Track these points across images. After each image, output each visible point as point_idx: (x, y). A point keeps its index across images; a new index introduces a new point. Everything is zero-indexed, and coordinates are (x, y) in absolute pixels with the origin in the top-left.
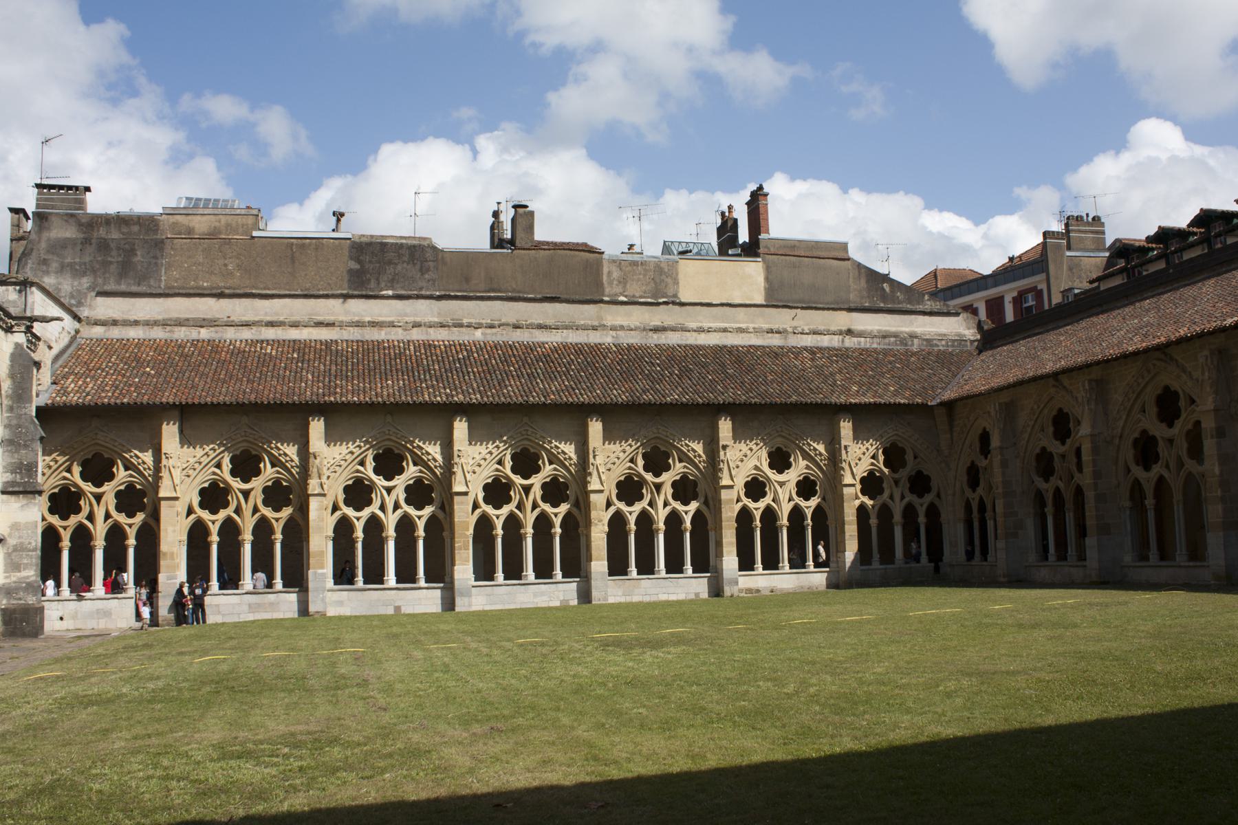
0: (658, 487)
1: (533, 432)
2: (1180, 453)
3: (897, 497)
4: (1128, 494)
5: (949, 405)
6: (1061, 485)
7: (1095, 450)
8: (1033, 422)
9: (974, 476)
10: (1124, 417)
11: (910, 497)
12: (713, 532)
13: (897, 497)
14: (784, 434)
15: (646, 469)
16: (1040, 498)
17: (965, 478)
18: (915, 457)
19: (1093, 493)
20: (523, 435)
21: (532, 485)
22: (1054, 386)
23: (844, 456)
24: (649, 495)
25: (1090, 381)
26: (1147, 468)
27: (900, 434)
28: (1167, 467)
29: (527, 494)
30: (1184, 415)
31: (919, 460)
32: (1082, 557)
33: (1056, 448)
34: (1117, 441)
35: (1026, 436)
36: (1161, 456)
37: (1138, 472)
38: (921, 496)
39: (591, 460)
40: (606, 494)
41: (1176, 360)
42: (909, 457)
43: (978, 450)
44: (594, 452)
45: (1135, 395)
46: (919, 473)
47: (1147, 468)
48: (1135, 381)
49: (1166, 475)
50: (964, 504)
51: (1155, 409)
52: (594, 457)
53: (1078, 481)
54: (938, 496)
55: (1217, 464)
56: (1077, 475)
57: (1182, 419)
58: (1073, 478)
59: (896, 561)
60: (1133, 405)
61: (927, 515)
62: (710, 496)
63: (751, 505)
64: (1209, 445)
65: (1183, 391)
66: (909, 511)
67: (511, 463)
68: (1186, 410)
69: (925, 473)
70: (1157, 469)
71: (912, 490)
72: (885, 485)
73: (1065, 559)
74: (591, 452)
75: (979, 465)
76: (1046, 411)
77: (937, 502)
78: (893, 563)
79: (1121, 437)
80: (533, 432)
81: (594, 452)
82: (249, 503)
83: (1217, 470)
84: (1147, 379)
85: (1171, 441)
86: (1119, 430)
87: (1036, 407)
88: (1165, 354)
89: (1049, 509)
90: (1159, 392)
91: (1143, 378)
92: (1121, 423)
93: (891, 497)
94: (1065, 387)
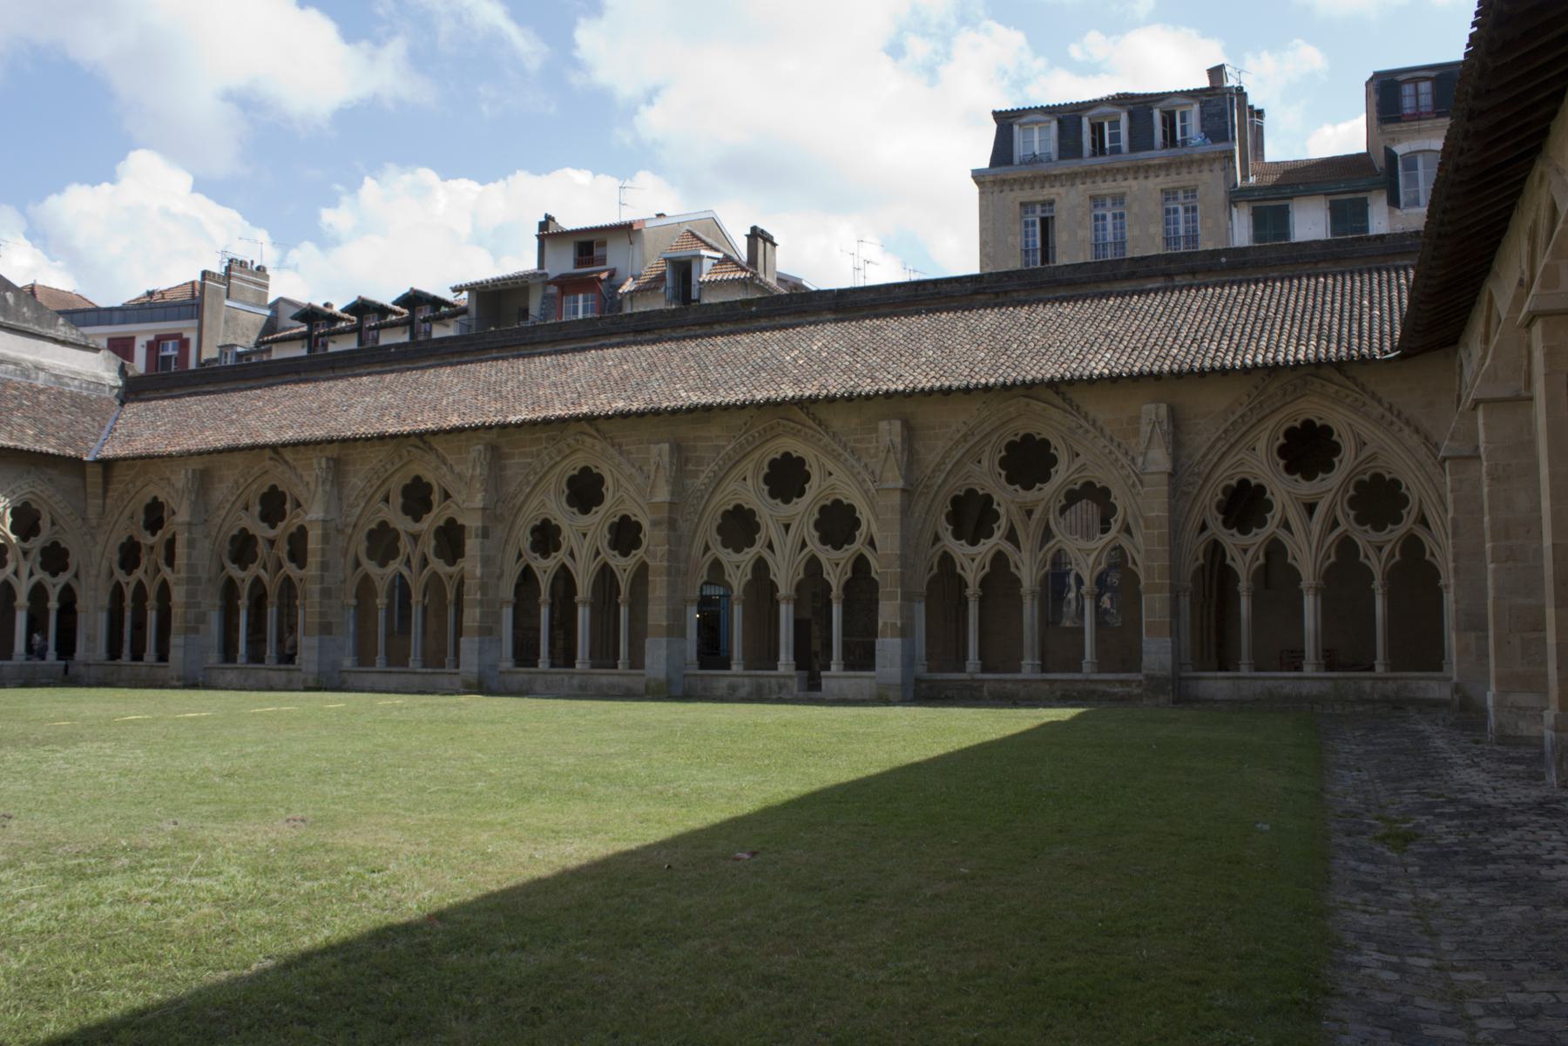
2: (426, 551)
3: (24, 572)
4: (354, 591)
5: (107, 465)
6: (265, 577)
7: (326, 538)
8: (234, 498)
9: (130, 555)
10: (362, 504)
11: (40, 575)
13: (24, 572)
17: (116, 557)
18: (53, 523)
19: (318, 586)
22: (271, 459)
25: (328, 459)
26: (383, 564)
27: (38, 492)
28: (408, 563)
30: (435, 510)
31: (57, 528)
33: (261, 531)
34: (349, 531)
35: (223, 513)
36: (402, 551)
37: (370, 567)
38: (54, 574)
41: (436, 450)
42: (45, 523)
43: (142, 523)
45: (380, 482)
46: (55, 544)
47: (383, 564)
48: (383, 466)
49: (406, 573)
50: (110, 589)
51: (400, 500)
53: (288, 572)
54: (76, 576)
55: (479, 565)
56: (290, 568)
57: (432, 515)
58: (281, 567)
59: (14, 657)
60: (376, 491)
61: (61, 598)
64: (472, 545)
65: (439, 484)
66: (38, 593)
68: (439, 506)
69: (63, 545)
70: (395, 566)
71: (44, 566)
72: (9, 556)
73: (262, 661)
75: (142, 541)
76: (254, 487)
77: (74, 584)
78: (10, 658)
79: (355, 526)
83: (478, 572)
84: (396, 466)
85: (415, 538)
86: (354, 519)
87: (242, 480)
88: (425, 442)
89: (243, 604)
90: (408, 481)
91: (393, 464)
92: (358, 511)
93: (16, 573)
94: (286, 462)
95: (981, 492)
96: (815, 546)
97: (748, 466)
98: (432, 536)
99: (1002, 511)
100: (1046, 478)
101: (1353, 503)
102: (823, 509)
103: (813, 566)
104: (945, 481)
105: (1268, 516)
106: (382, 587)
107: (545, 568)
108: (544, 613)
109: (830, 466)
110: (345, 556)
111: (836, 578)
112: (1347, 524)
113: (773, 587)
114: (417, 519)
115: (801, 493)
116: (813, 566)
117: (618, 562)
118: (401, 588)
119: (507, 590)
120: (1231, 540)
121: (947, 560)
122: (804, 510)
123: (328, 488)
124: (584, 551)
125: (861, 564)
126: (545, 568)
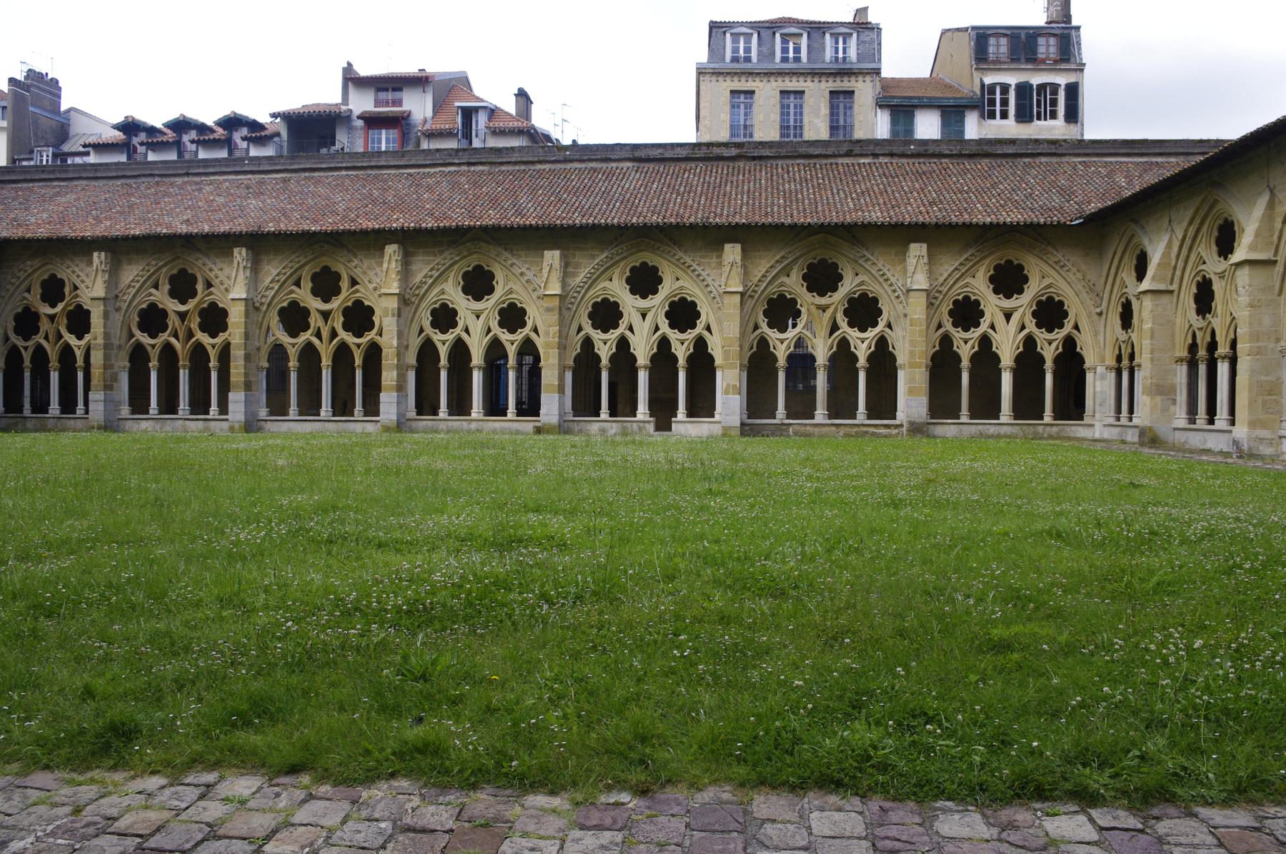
16: (138, 356)
30: (344, 294)
32: (223, 408)
79: (269, 305)
85: (326, 315)
95: (789, 297)
96: (665, 328)
97: (617, 272)
98: (340, 314)
99: (803, 310)
100: (835, 289)
101: (1034, 314)
102: (672, 304)
103: (664, 343)
104: (765, 288)
105: (982, 320)
106: (293, 353)
107: (443, 342)
108: (443, 375)
109: (680, 273)
110: (260, 328)
111: (681, 352)
112: (1031, 327)
113: (633, 359)
114: (326, 300)
115: (655, 292)
116: (664, 343)
117: (505, 336)
118: (309, 353)
119: (412, 358)
120: (958, 335)
121: (763, 342)
122: (658, 302)
123: (248, 274)
124: (477, 327)
125: (701, 344)
126: (443, 342)
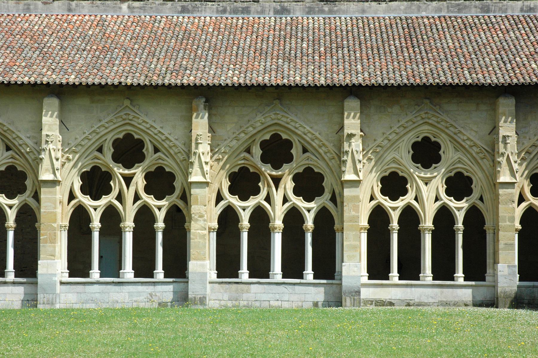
0: (277, 181)
1: (134, 117)
12: (340, 233)
14: (430, 121)
15: (264, 159)
20: (124, 120)
21: (135, 174)
23: (502, 150)
24: (266, 188)
29: (128, 183)
39: (193, 150)
40: (215, 187)
44: (197, 139)
52: (197, 144)
62: (337, 192)
63: (387, 203)
67: (112, 150)
74: (193, 139)
80: (134, 117)
81: (197, 139)
82: (130, 188)
